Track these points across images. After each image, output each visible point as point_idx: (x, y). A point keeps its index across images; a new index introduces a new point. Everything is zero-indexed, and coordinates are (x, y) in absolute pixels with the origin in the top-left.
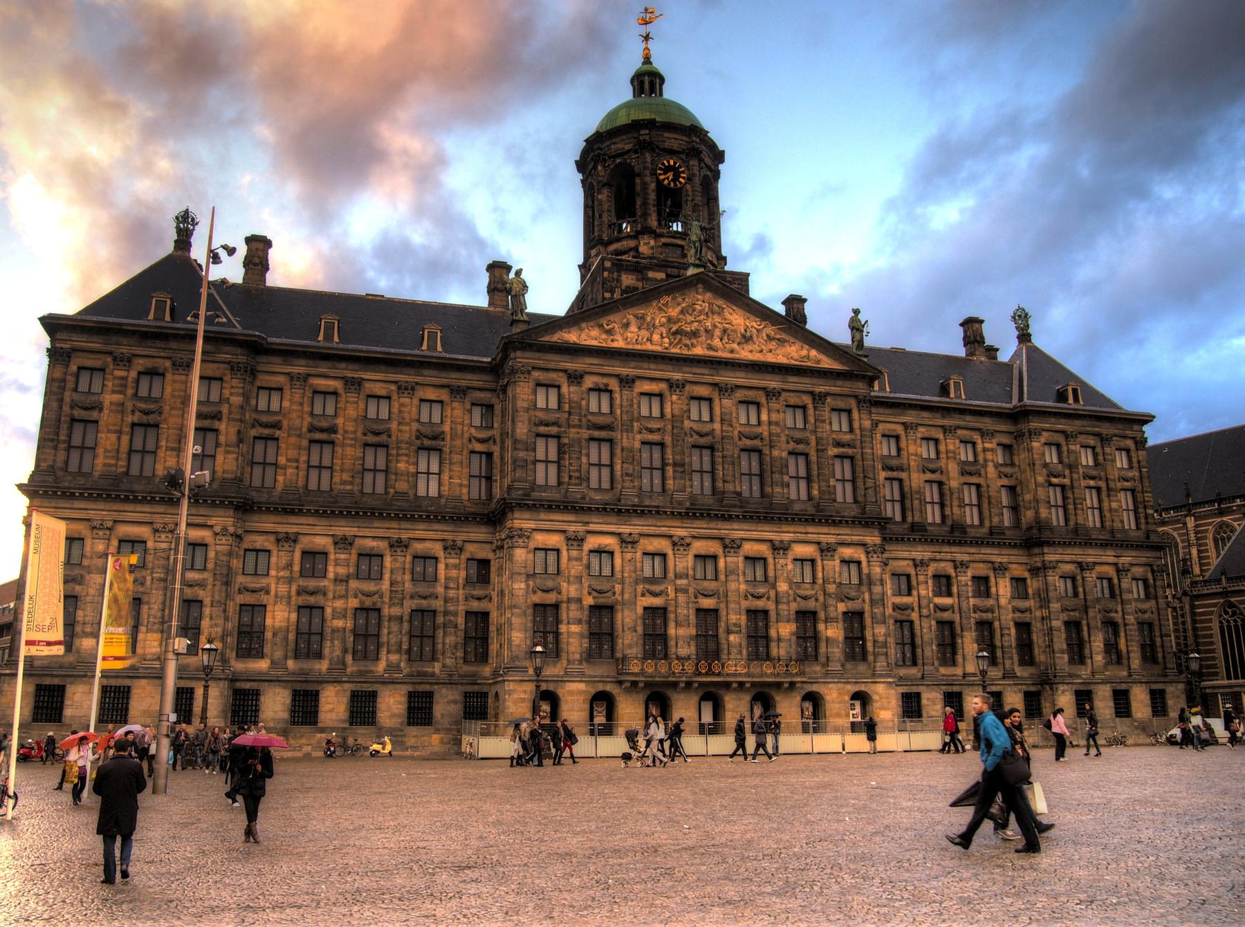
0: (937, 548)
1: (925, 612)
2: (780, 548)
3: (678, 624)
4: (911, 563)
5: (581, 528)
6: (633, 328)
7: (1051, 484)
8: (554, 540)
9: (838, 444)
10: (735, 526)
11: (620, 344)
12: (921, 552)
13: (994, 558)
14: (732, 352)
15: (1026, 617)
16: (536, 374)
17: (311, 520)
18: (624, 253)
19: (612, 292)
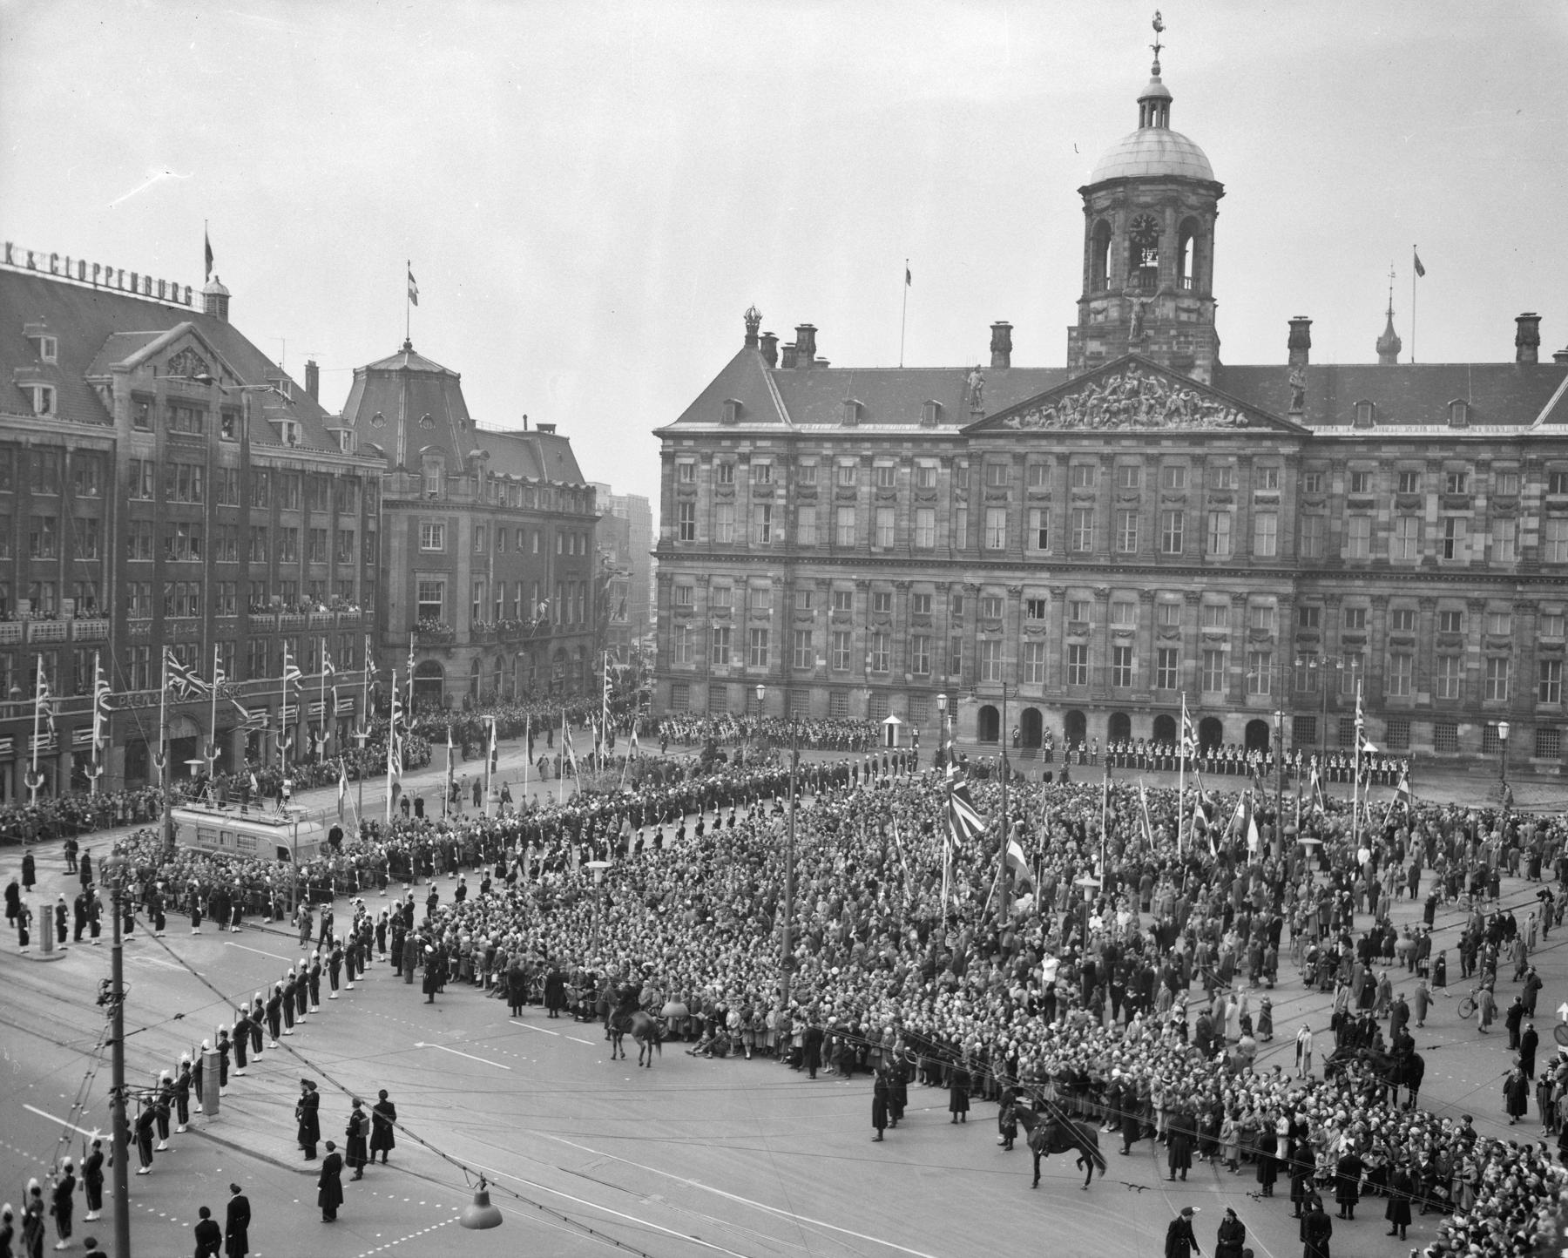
0: (1401, 584)
1: (1378, 646)
2: (1194, 599)
3: (1096, 658)
4: (1368, 599)
5: (1020, 583)
6: (1069, 411)
7: (1549, 518)
8: (1001, 592)
9: (1259, 500)
10: (1151, 578)
11: (1056, 429)
12: (1381, 588)
13: (1470, 594)
14: (1157, 424)
15: (1504, 653)
16: (987, 456)
17: (840, 568)
18: (1098, 312)
19: (1076, 360)
